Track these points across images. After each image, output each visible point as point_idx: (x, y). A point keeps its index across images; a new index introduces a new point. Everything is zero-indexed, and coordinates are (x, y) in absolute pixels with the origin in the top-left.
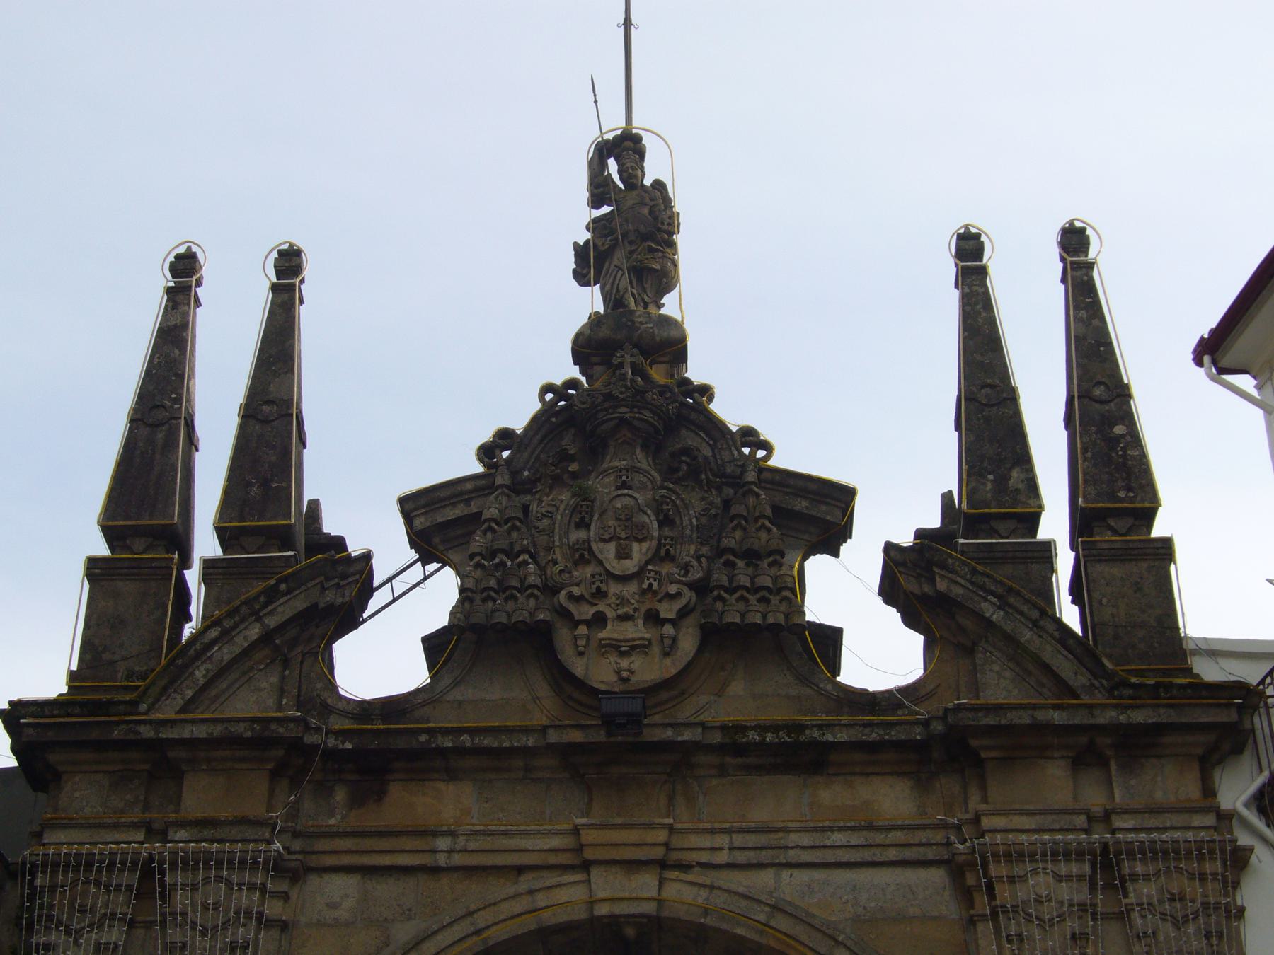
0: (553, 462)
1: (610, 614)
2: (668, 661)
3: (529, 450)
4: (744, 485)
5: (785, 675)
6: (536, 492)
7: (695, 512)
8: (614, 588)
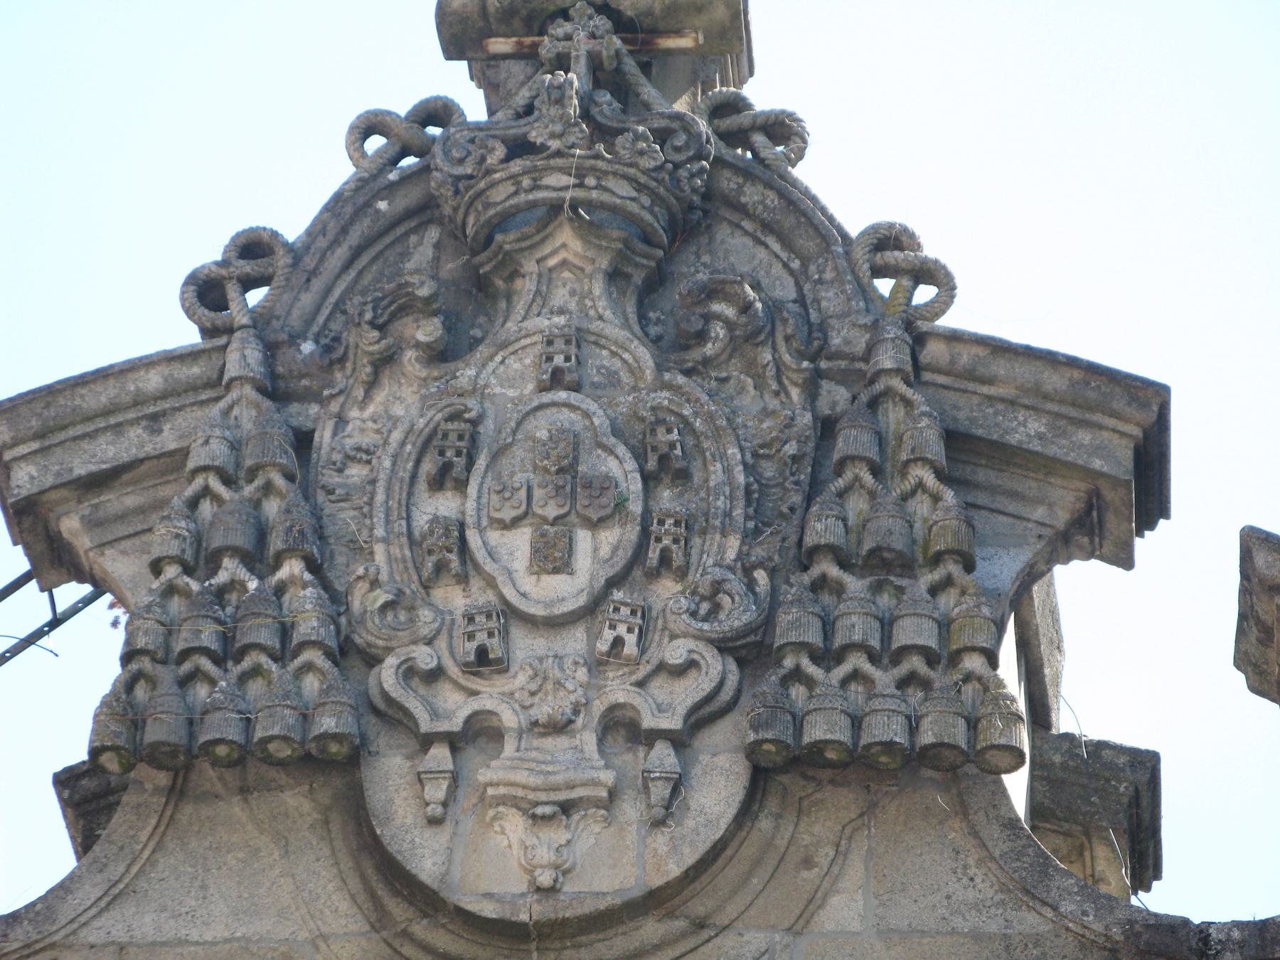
0: (375, 317)
1: (509, 718)
2: (660, 841)
3: (317, 285)
4: (872, 382)
5: (972, 879)
6: (333, 396)
7: (742, 449)
8: (525, 645)
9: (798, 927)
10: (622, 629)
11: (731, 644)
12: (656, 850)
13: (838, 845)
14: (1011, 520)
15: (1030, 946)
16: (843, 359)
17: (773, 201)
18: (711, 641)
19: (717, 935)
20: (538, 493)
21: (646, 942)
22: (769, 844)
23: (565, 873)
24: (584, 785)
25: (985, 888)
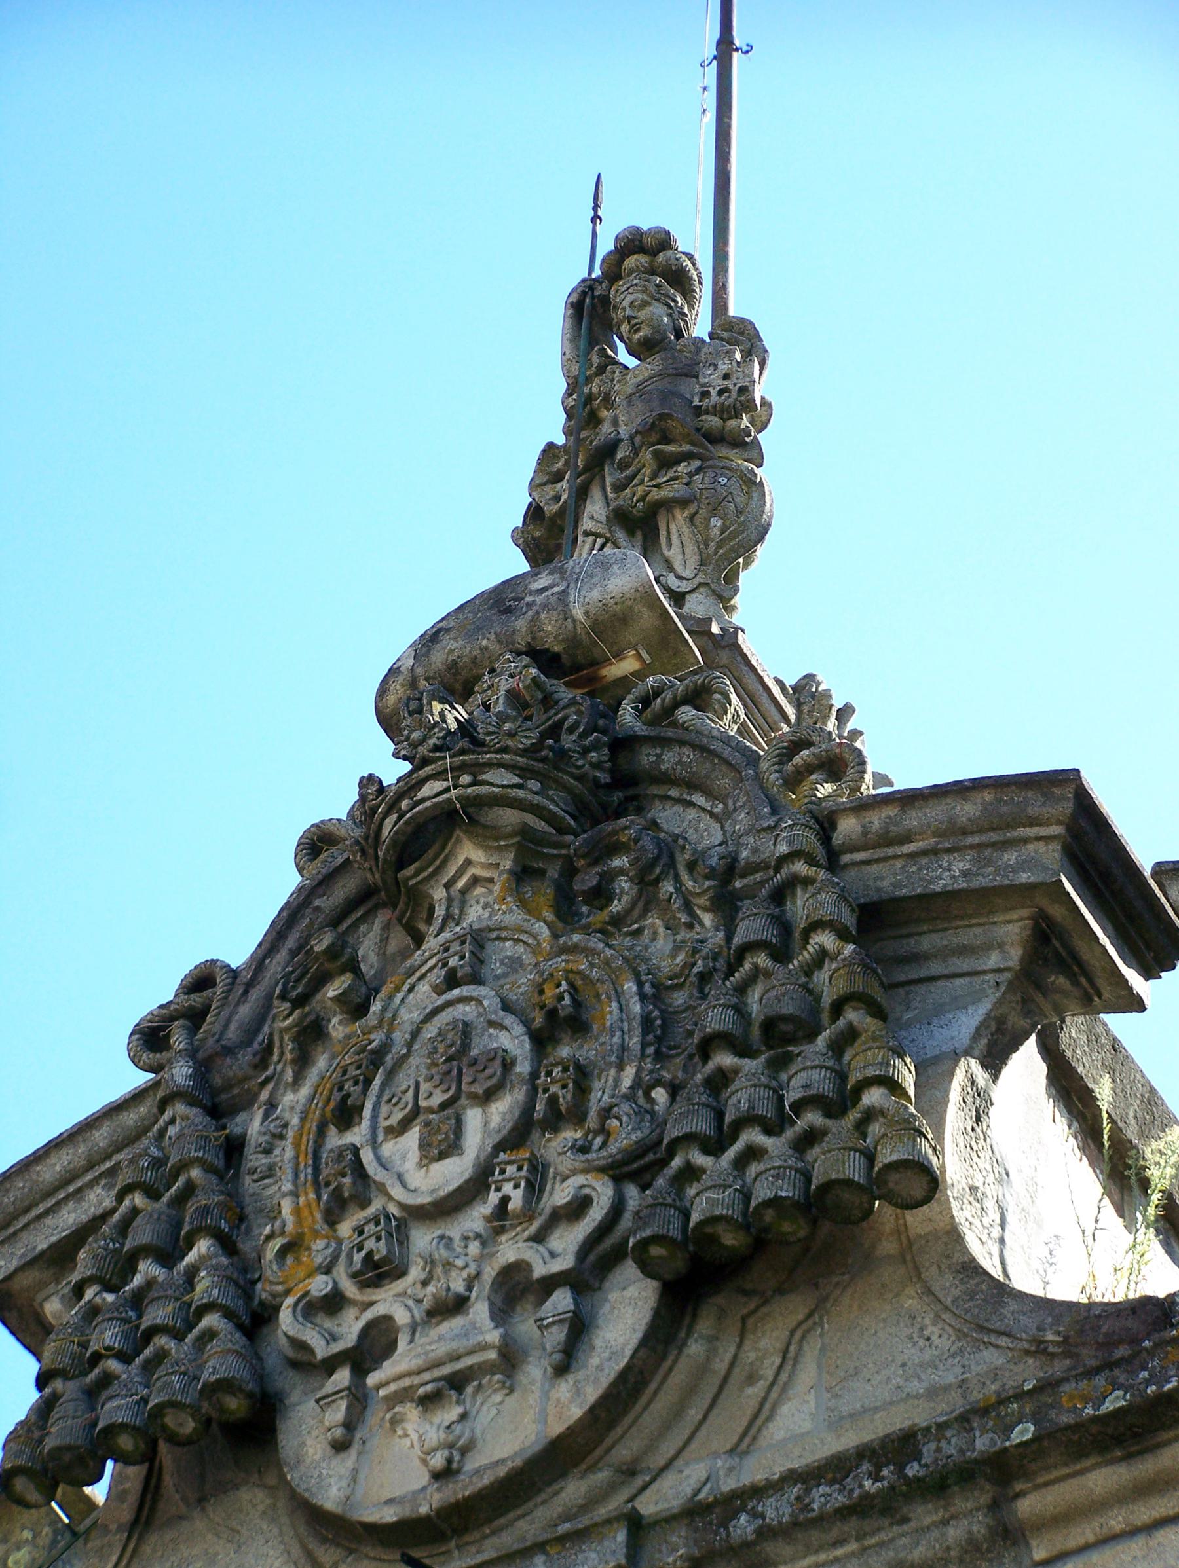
1: (402, 1317)
2: (563, 1389)
5: (928, 1339)
8: (422, 1239)
9: (743, 1446)
10: (508, 1188)
11: (626, 1169)
12: (558, 1400)
13: (785, 1352)
14: (968, 979)
15: (988, 1383)
16: (757, 872)
17: (688, 756)
18: (602, 1170)
19: (653, 1480)
20: (425, 1087)
21: (569, 1504)
22: (702, 1370)
23: (464, 1451)
24: (470, 1353)
25: (943, 1341)
